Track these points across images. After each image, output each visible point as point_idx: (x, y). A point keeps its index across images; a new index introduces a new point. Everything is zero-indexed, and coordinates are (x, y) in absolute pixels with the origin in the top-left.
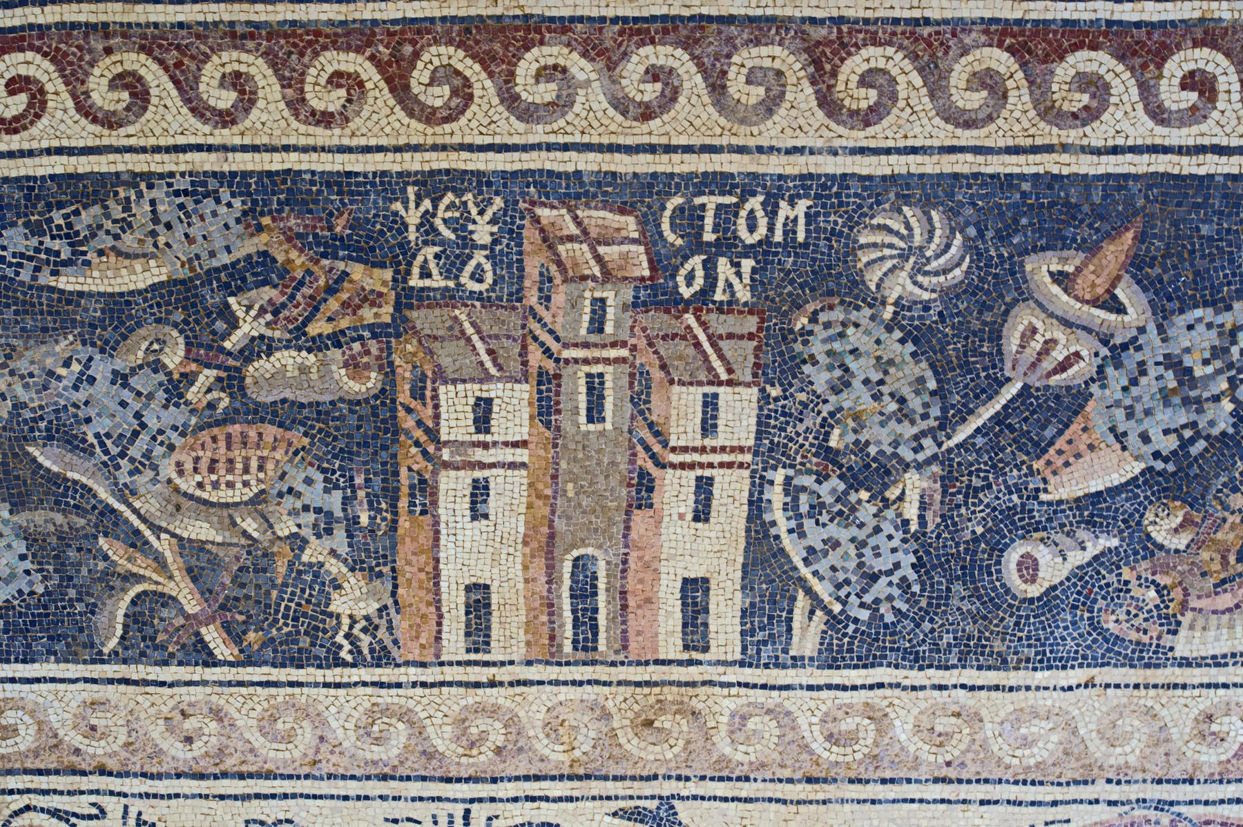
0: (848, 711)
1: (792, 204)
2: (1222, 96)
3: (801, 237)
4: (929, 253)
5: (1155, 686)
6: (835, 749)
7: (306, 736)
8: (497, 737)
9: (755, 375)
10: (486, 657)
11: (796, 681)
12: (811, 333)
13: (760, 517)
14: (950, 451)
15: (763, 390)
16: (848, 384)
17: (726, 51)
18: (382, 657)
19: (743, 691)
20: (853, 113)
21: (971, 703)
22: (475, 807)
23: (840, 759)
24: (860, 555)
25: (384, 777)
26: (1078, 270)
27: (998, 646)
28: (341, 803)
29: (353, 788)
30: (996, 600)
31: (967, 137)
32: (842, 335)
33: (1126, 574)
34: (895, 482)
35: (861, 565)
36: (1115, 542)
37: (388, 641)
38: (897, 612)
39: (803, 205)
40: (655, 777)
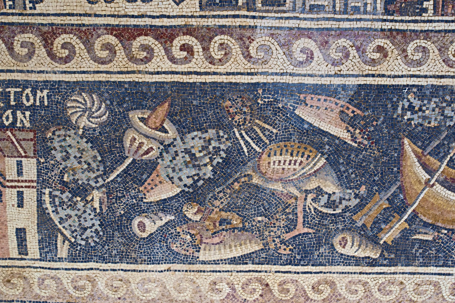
0: (81, 278)
1: (42, 92)
2: (196, 53)
3: (46, 103)
4: (93, 110)
5: (193, 271)
6: (77, 292)
9: (34, 154)
11: (61, 267)
12: (53, 139)
13: (41, 206)
14: (108, 183)
15: (38, 160)
16: (68, 158)
17: (12, 35)
19: (42, 270)
20: (61, 58)
21: (126, 276)
23: (80, 296)
24: (80, 221)
26: (149, 117)
27: (133, 255)
30: (131, 238)
31: (103, 68)
32: (65, 140)
33: (178, 230)
34: (90, 194)
35: (80, 224)
36: (173, 218)
38: (95, 242)
39: (45, 92)
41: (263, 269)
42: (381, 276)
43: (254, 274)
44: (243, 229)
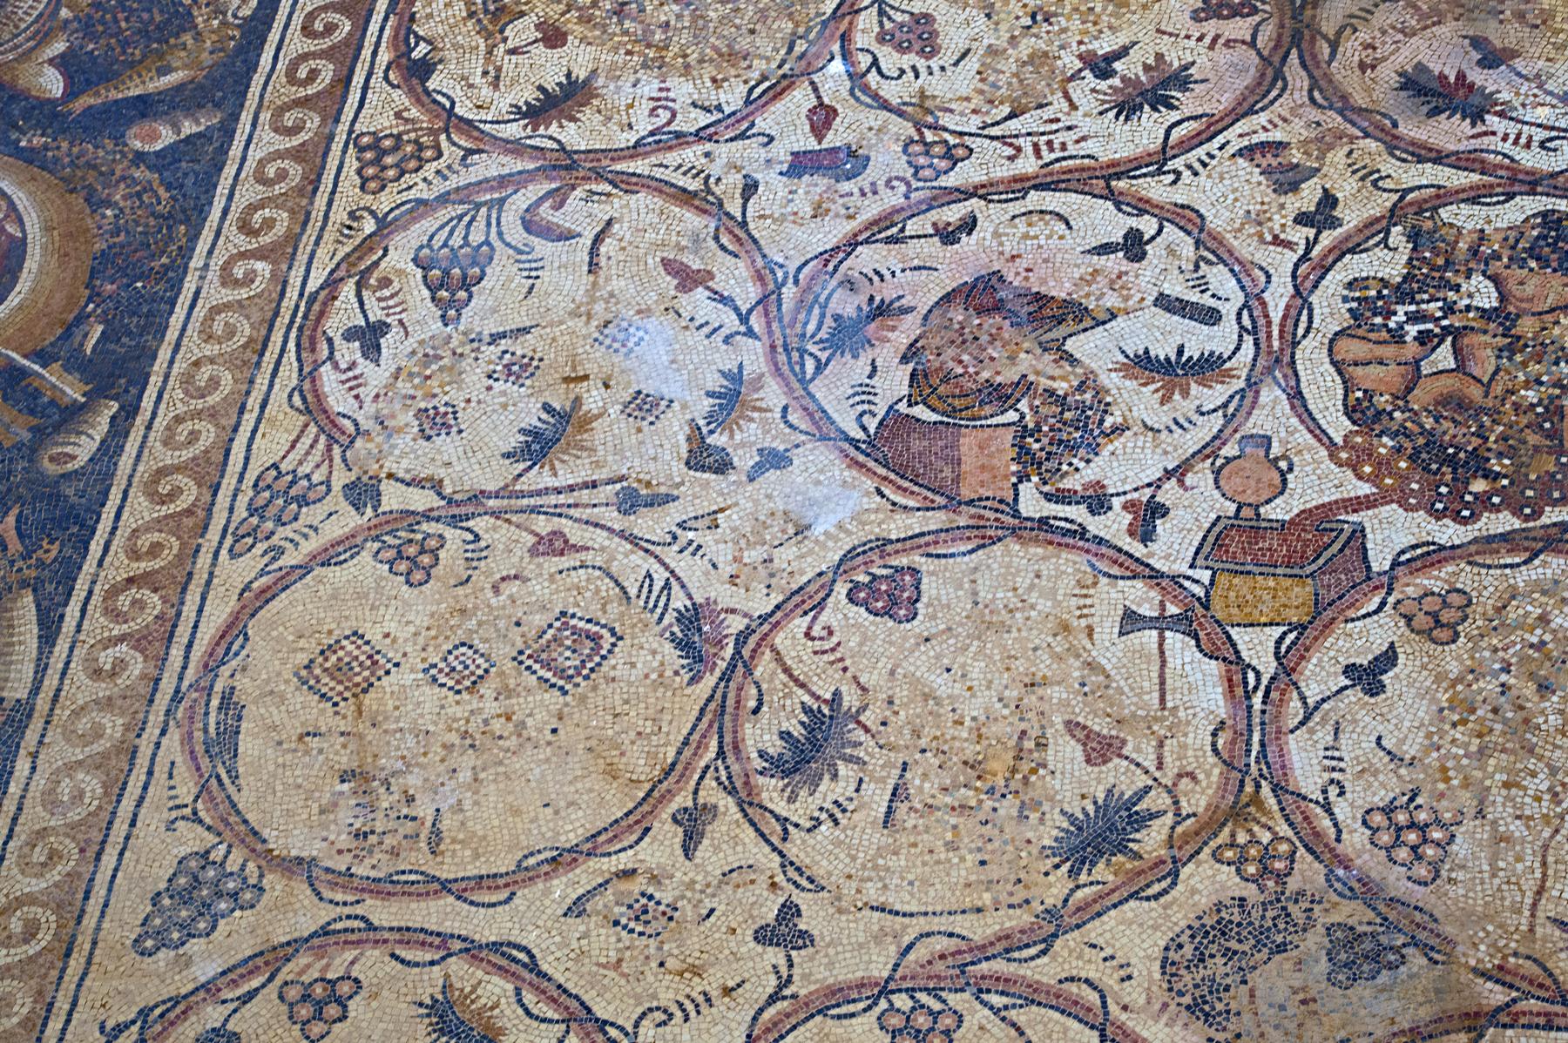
5: (52, 710)
6: (39, 936)
21: (23, 837)
41: (86, 587)
42: (166, 396)
43: (92, 602)
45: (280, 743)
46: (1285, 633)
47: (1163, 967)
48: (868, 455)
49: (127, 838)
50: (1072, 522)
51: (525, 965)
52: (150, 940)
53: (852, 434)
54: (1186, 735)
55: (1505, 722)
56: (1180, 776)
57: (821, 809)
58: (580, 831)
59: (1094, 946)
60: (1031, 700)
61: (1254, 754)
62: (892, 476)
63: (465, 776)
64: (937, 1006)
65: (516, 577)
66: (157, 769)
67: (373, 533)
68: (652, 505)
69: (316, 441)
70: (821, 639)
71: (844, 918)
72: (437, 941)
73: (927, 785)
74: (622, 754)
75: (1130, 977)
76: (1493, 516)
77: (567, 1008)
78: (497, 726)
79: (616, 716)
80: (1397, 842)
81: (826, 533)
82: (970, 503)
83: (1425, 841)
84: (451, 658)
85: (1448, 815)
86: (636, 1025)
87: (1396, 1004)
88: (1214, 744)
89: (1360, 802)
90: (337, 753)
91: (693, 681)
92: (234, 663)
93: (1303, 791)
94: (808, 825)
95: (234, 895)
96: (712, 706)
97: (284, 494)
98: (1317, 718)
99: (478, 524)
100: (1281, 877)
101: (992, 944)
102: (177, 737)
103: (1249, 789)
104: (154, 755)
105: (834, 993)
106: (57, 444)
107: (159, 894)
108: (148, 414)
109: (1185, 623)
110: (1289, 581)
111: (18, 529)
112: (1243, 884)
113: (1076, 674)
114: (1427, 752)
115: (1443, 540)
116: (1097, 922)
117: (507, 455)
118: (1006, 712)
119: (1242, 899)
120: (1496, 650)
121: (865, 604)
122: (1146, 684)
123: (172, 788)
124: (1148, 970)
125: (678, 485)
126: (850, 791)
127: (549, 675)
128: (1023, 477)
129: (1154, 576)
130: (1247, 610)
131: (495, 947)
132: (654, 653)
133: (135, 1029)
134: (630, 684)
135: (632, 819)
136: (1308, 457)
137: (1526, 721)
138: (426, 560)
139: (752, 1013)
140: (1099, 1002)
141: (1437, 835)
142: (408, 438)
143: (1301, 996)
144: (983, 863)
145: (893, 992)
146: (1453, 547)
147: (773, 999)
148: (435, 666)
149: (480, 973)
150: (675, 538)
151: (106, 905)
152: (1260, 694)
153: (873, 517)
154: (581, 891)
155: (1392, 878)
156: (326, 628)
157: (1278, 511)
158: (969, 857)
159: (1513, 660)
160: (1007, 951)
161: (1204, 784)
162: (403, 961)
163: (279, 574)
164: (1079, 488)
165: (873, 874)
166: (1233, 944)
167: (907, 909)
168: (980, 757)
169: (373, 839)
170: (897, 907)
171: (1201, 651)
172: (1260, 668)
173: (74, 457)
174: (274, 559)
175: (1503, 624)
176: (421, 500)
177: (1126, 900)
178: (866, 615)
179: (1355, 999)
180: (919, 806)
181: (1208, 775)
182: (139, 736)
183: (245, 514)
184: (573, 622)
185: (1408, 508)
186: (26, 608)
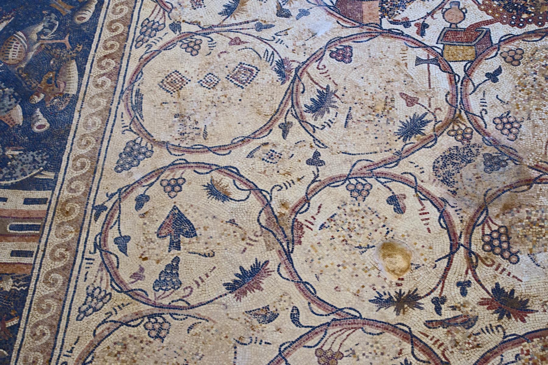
0: (73, 165)
7: (50, 301)
8: (62, 250)
10: (35, 252)
11: (62, 177)
18: (28, 279)
19: (62, 190)
21: (78, 137)
22: (85, 257)
24: (27, 164)
25: (70, 281)
27: (63, 132)
28: (76, 293)
29: (71, 290)
30: (48, 133)
33: (49, 106)
34: (7, 157)
35: (30, 163)
36: (38, 109)
37: (23, 277)
38: (46, 155)
40: (85, 211)
44: (58, 71)
45: (155, 106)
46: (467, 64)
47: (433, 168)
48: (333, 11)
49: (110, 136)
50: (399, 30)
51: (236, 173)
52: (120, 168)
53: (328, 4)
54: (437, 96)
55: (536, 89)
56: (436, 109)
57: (325, 122)
58: (250, 131)
59: (412, 163)
60: (389, 87)
61: (459, 102)
62: (342, 17)
63: (213, 115)
64: (364, 182)
65: (225, 52)
66: (117, 115)
67: (180, 39)
68: (266, 28)
69: (160, 11)
70: (322, 69)
71: (334, 156)
72: (208, 166)
73: (358, 114)
74: (262, 107)
75: (423, 172)
76: (529, 25)
77: (249, 186)
78: (222, 99)
79: (259, 95)
80: (504, 128)
81: (322, 36)
82: (367, 25)
83: (512, 127)
84: (206, 78)
85: (519, 119)
86: (271, 191)
87: (505, 178)
88: (446, 99)
89: (492, 116)
90: (173, 109)
91: (283, 83)
92: (139, 82)
93: (474, 113)
94: (321, 127)
95: (144, 154)
96: (289, 91)
97: (151, 28)
98: (478, 90)
99: (212, 36)
100: (468, 140)
101: (380, 163)
102: (123, 105)
103: (458, 112)
104: (117, 110)
105: (332, 179)
106: (79, 14)
107: (121, 154)
108: (107, 4)
109: (436, 61)
110: (467, 48)
111: (69, 41)
112: (457, 142)
113: (403, 78)
114: (512, 100)
115: (514, 33)
116: (412, 155)
117: (220, 14)
118: (381, 91)
119: (457, 147)
120: (532, 67)
121: (335, 58)
122: (424, 81)
123: (123, 121)
124: (429, 169)
125: (274, 22)
126: (334, 117)
127: (237, 83)
128: (383, 16)
129: (426, 47)
130: (455, 57)
131: (226, 168)
132: (270, 75)
133: (117, 195)
134: (263, 85)
135: (266, 127)
136: (471, 8)
137: (542, 89)
138: (196, 47)
139: (307, 186)
140: (414, 180)
141: (516, 125)
142: (189, 9)
143: (476, 176)
144: (376, 138)
145: (350, 178)
146: (518, 35)
147: (313, 181)
148: (201, 81)
149: (222, 176)
150: (274, 38)
151: (105, 157)
152: (460, 83)
153: (336, 30)
154: (252, 150)
155: (502, 139)
156: (167, 69)
157: (464, 25)
158: (372, 136)
159: (538, 70)
160: (385, 165)
161: (444, 111)
162: (198, 173)
163: (151, 53)
164: (400, 19)
165: (342, 142)
166: (455, 161)
167: (353, 153)
168: (374, 105)
169: (186, 135)
170: (350, 152)
171: (441, 70)
172: (459, 75)
173: (85, 18)
174: (149, 48)
175: (534, 59)
176: (194, 28)
177: (421, 148)
178: (336, 61)
179: (492, 177)
180: (355, 121)
181: (445, 108)
182: (111, 105)
183: (139, 34)
184: (244, 66)
185: (503, 24)
186: (73, 66)
